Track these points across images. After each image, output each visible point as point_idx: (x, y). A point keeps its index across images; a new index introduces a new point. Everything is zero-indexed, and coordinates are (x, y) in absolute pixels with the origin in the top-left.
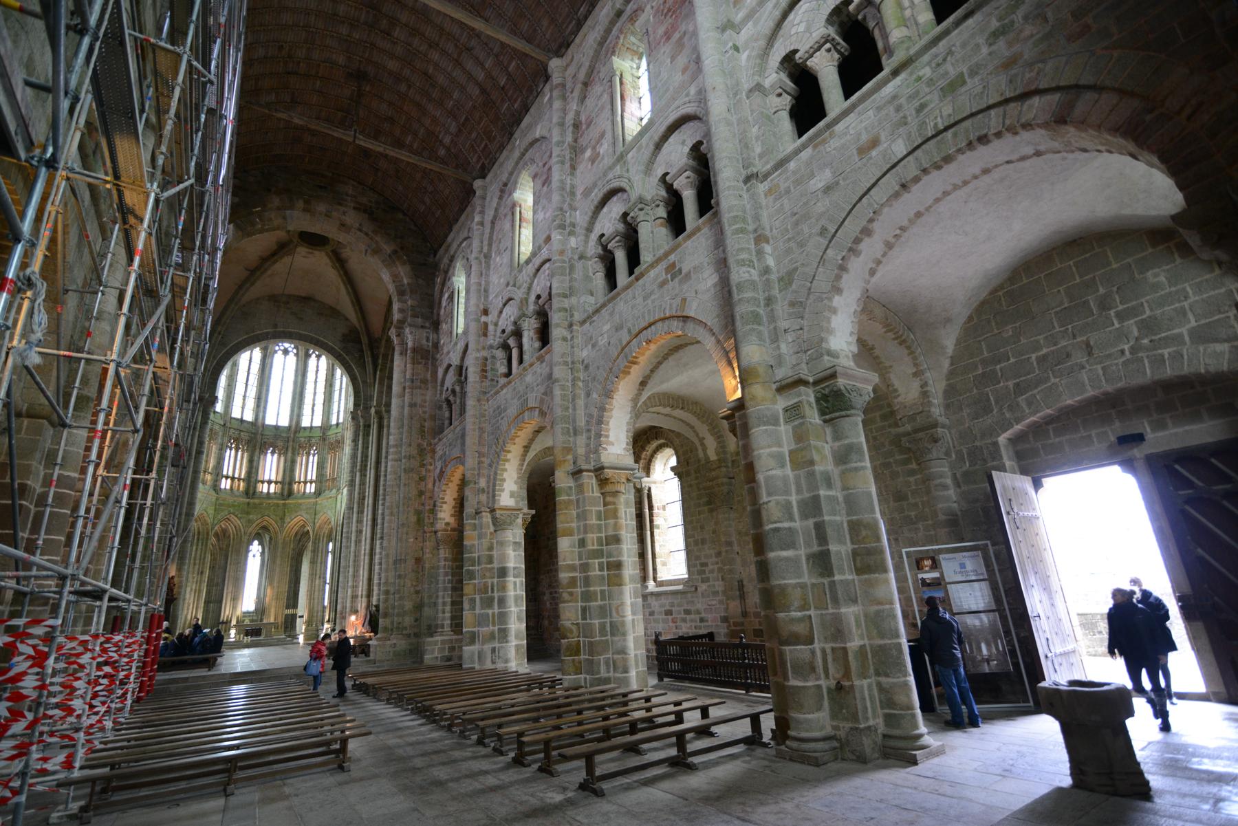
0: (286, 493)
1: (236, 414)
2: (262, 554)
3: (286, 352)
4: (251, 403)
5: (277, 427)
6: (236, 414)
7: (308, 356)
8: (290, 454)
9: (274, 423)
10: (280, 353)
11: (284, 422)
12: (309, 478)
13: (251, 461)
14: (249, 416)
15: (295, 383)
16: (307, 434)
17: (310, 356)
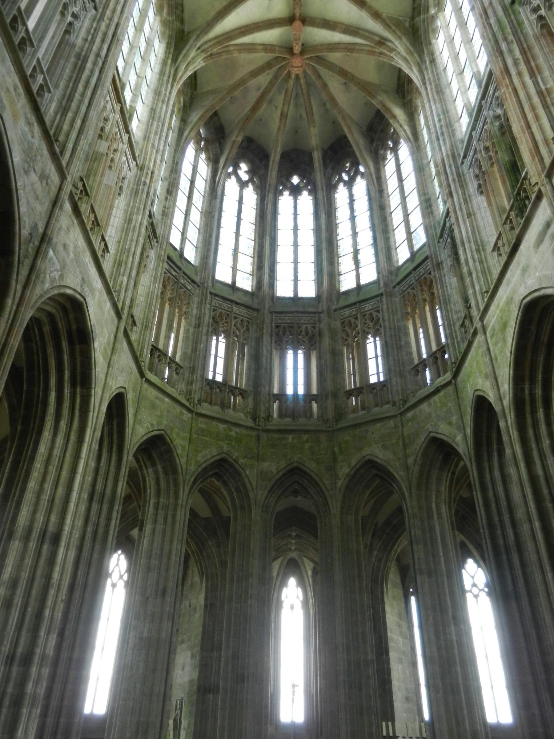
0: (330, 414)
1: (223, 274)
2: (305, 603)
3: (295, 191)
4: (246, 264)
5: (296, 299)
6: (223, 274)
7: (331, 188)
8: (326, 341)
9: (292, 295)
10: (286, 193)
11: (308, 290)
12: (373, 380)
13: (256, 358)
14: (245, 283)
15: (317, 230)
16: (352, 299)
17: (335, 187)
